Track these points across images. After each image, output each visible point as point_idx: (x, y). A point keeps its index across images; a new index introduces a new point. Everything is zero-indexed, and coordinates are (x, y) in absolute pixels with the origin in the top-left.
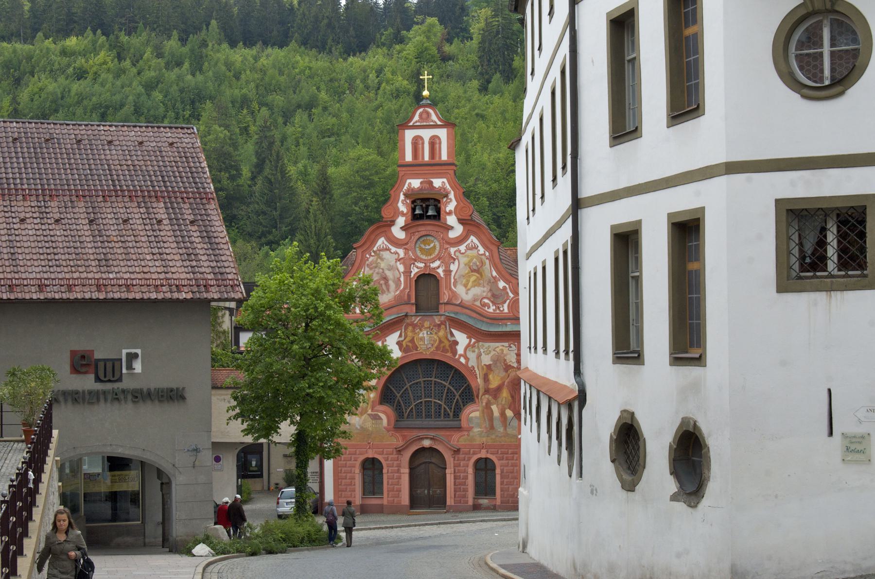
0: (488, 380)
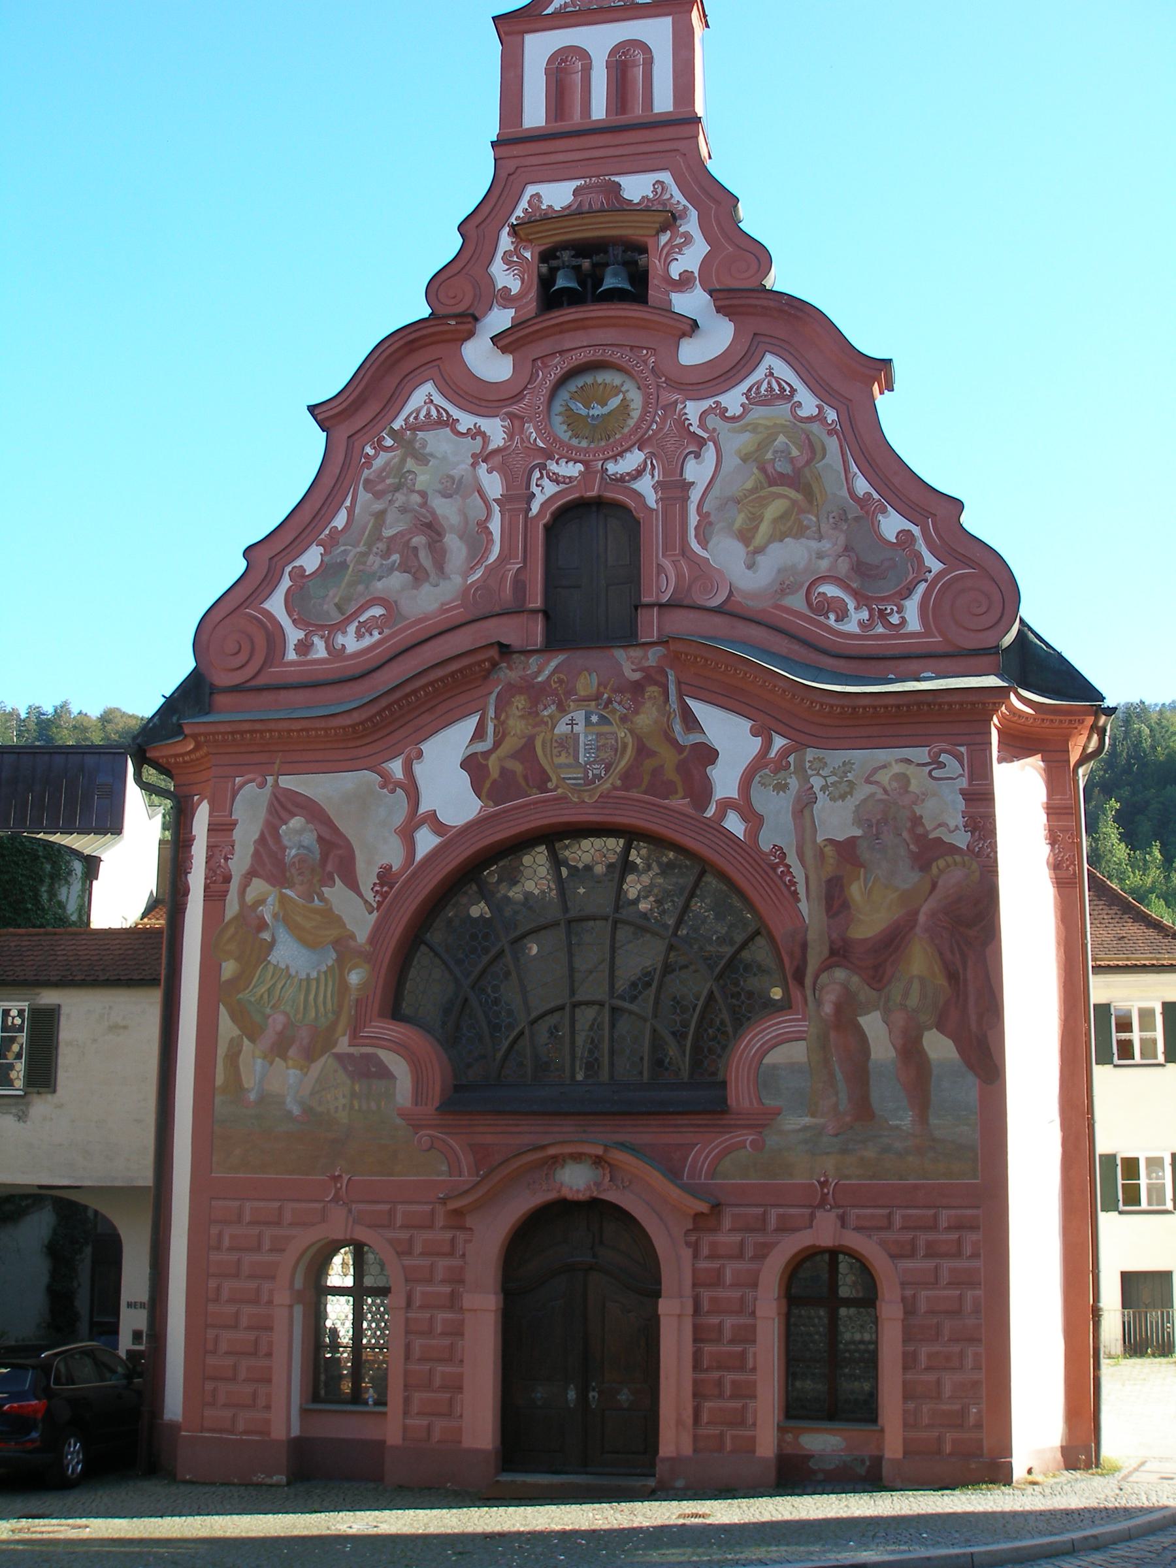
0: (845, 905)
